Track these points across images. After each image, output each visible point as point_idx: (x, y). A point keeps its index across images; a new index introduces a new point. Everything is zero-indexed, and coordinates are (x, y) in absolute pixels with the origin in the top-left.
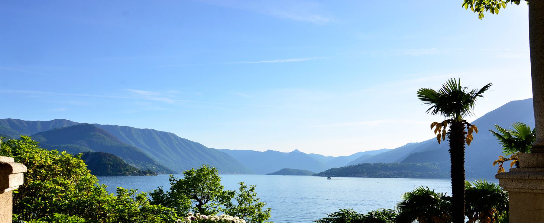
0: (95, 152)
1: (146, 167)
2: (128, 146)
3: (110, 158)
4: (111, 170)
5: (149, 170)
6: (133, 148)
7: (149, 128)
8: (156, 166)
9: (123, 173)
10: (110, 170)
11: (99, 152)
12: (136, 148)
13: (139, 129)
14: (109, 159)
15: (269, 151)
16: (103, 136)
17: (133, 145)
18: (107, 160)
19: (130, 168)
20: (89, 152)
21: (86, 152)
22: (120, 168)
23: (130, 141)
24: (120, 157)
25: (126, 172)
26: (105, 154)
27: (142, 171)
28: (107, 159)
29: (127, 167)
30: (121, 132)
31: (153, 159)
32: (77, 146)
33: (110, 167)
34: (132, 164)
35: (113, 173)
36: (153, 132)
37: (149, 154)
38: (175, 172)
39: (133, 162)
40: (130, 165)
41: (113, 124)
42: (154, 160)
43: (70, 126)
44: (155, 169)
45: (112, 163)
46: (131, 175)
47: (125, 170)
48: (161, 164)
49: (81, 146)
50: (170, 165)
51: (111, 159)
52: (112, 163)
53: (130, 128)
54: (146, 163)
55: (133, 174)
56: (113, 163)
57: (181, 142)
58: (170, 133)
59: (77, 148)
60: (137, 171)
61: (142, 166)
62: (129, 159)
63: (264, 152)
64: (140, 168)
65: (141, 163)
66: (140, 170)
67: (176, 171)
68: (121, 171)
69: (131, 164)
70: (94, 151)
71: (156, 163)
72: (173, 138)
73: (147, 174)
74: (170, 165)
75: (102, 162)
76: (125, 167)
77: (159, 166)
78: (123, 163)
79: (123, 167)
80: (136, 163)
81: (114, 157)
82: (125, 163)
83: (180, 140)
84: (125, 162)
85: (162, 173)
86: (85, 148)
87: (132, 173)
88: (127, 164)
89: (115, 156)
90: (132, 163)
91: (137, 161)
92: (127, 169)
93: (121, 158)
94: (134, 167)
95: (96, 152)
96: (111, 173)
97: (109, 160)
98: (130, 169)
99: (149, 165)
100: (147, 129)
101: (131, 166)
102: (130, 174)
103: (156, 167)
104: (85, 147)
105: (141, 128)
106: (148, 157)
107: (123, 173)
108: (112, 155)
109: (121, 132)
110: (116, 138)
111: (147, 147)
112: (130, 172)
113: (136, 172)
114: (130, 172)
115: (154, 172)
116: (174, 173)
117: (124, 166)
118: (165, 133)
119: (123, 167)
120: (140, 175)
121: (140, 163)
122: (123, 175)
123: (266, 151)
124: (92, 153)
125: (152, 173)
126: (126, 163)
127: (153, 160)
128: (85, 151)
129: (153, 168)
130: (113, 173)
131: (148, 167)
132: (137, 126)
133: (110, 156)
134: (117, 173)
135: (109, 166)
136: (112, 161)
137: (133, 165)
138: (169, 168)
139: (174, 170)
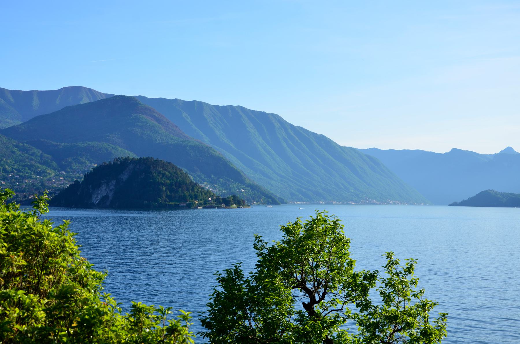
0: (139, 158)
1: (230, 190)
2: (197, 143)
3: (166, 170)
4: (167, 196)
5: (234, 196)
6: (207, 147)
7: (235, 104)
8: (248, 186)
9: (188, 202)
10: (165, 197)
11: (145, 157)
12: (211, 148)
13: (217, 107)
14: (164, 172)
15: (454, 151)
16: (154, 122)
17: (206, 141)
18: (161, 176)
19: (201, 191)
20: (127, 159)
21: (122, 158)
22: (183, 192)
23: (201, 133)
24: (183, 169)
25: (193, 200)
26: (156, 163)
27: (223, 199)
28: (159, 172)
29: (196, 191)
30: (184, 115)
31: (243, 172)
32: (106, 145)
33: (166, 190)
34: (205, 183)
35: (170, 203)
36: (241, 113)
37: (236, 163)
38: (282, 199)
39: (206, 179)
40: (200, 185)
41: (170, 96)
42: (243, 175)
43: (93, 101)
44: (244, 194)
45: (168, 182)
46: (203, 208)
47: (191, 197)
48: (256, 183)
49: (112, 145)
50: (272, 185)
51: (167, 173)
52: (168, 182)
53: (200, 104)
54: (229, 181)
55: (206, 205)
56: (170, 180)
57: (292, 133)
58: (273, 115)
59: (107, 150)
60: (212, 199)
61: (222, 187)
62: (199, 173)
63: (445, 153)
64: (218, 191)
65: (221, 180)
66: (219, 197)
67: (282, 197)
68: (184, 199)
69: (203, 183)
70: (136, 157)
71: (247, 181)
72: (277, 125)
73: (232, 206)
74: (272, 185)
75: (151, 181)
76: (193, 190)
77: (253, 187)
78: (188, 182)
79: (189, 191)
80: (212, 182)
81: (173, 168)
82: (192, 181)
83: (290, 131)
84: (192, 178)
85: (259, 202)
86: (120, 149)
87: (205, 203)
88: (196, 184)
89: (174, 167)
90: (204, 181)
91: (213, 176)
92: (195, 195)
93: (185, 170)
94: (208, 191)
95: (141, 158)
96: (167, 203)
97: (164, 175)
98: (202, 194)
99: (235, 185)
100: (231, 106)
101: (202, 188)
102: (200, 205)
103: (248, 190)
104: (121, 147)
105: (221, 105)
106: (233, 168)
107: (188, 202)
108: (169, 163)
109: (184, 115)
110: (177, 127)
111: (231, 145)
112: (201, 200)
113: (212, 202)
114: (202, 202)
115: (243, 201)
116: (279, 202)
117: (191, 188)
118: (263, 115)
119: (188, 190)
120: (218, 207)
121: (219, 181)
122: (189, 206)
123: (448, 152)
124: (133, 159)
125: (239, 203)
126: (194, 182)
127: (242, 174)
128: (120, 157)
129: (241, 192)
130: (170, 203)
131: (233, 191)
132: (213, 101)
133: (164, 165)
134: (177, 203)
135: (164, 189)
136: (168, 178)
137: (207, 186)
138: (271, 192)
139: (278, 196)
